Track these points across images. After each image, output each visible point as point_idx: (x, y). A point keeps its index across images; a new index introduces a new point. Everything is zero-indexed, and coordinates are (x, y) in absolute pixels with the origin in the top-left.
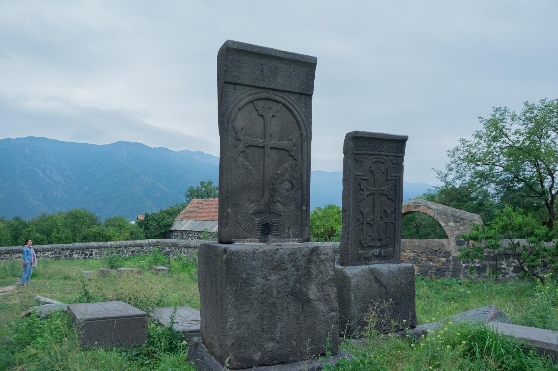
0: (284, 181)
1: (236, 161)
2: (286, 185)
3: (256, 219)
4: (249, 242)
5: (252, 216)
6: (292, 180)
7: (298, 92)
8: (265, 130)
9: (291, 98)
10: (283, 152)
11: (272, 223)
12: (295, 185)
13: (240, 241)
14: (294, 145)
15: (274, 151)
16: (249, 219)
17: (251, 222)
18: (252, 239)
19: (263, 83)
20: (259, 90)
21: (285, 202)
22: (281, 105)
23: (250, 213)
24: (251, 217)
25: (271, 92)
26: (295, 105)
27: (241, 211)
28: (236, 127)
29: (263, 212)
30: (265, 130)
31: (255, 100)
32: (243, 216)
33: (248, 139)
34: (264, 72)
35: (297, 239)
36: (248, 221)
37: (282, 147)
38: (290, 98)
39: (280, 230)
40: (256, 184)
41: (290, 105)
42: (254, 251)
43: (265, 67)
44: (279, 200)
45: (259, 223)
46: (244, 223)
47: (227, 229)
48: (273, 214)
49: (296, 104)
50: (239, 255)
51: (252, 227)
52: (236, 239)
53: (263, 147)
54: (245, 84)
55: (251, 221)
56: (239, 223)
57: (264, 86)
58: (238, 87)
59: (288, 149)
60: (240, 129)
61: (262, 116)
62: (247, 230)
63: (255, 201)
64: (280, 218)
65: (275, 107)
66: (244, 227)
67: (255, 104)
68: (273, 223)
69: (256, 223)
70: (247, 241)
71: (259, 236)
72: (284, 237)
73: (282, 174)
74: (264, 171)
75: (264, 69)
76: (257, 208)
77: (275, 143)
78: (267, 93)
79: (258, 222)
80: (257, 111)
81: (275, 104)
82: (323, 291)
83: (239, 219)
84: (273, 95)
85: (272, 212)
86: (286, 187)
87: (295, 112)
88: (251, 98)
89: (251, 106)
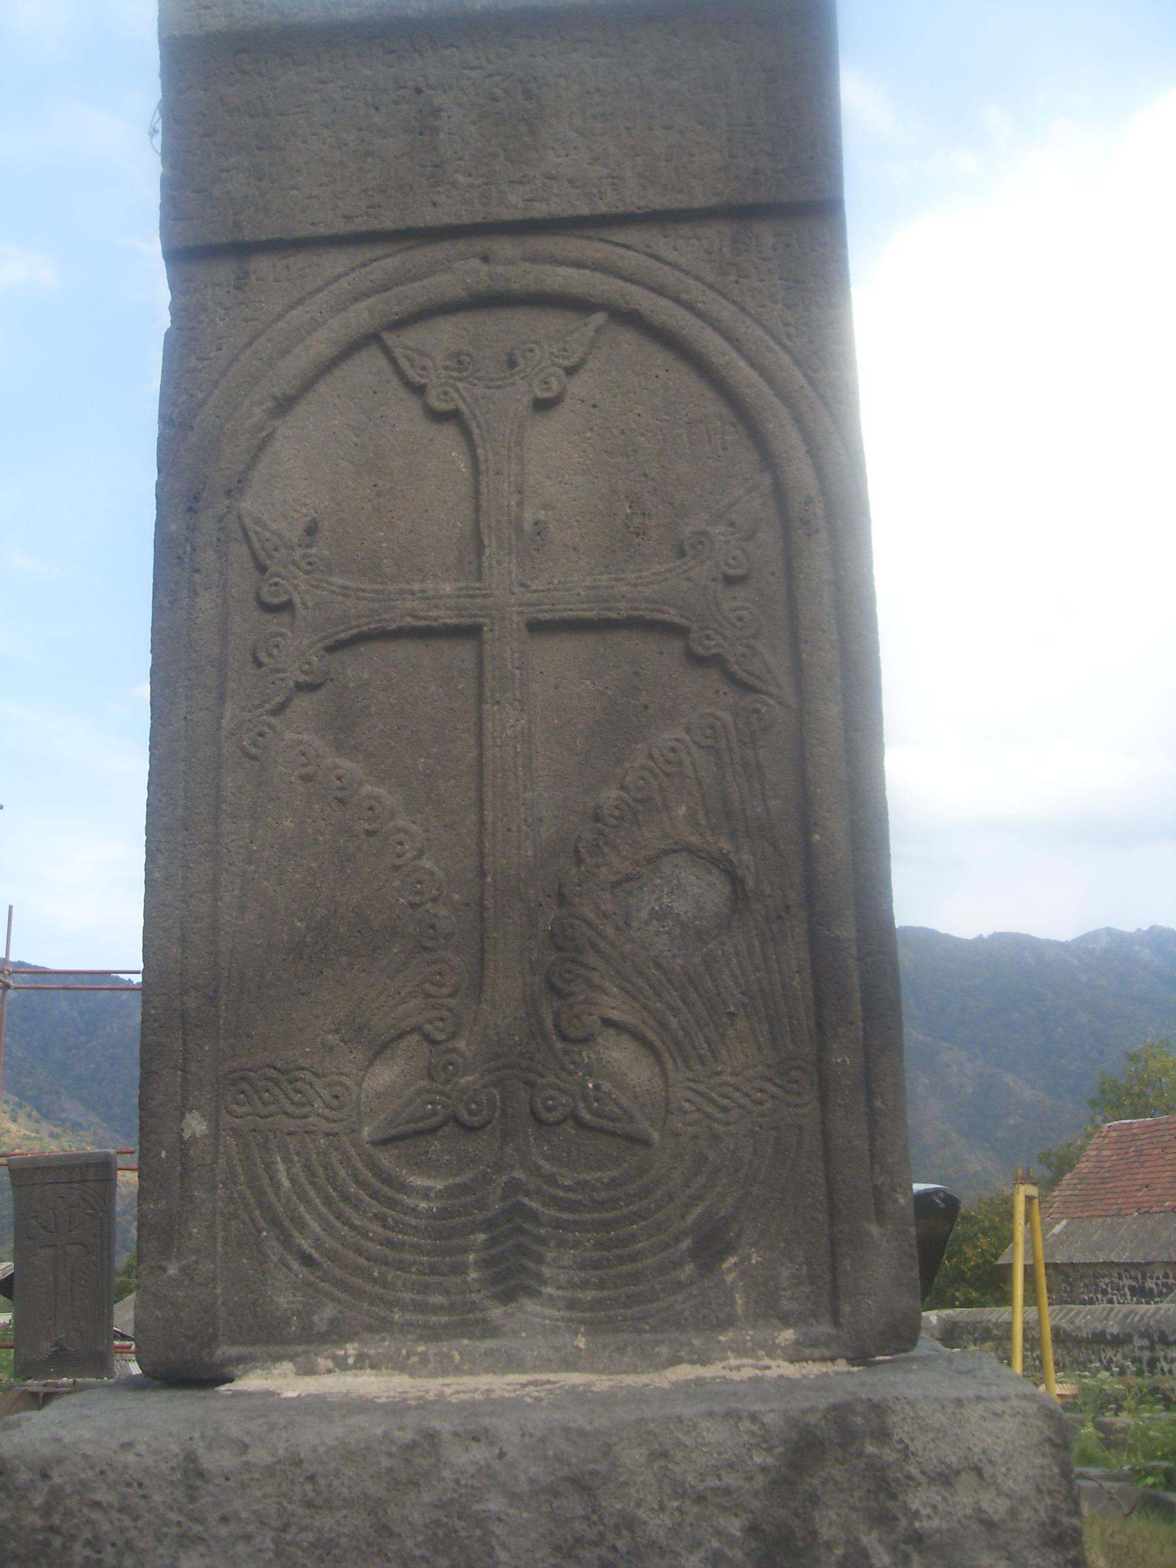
0: (653, 861)
1: (254, 758)
3: (419, 1181)
4: (355, 1367)
5: (385, 1159)
6: (726, 846)
7: (713, 201)
8: (477, 509)
9: (670, 255)
11: (558, 1203)
12: (750, 884)
13: (280, 1358)
14: (730, 581)
15: (568, 647)
16: (362, 1184)
17: (377, 1207)
18: (385, 1345)
19: (442, 199)
20: (420, 256)
21: (664, 1026)
22: (600, 318)
23: (366, 1132)
24: (373, 1166)
25: (504, 247)
27: (292, 1125)
28: (258, 521)
29: (475, 1121)
30: (477, 509)
31: (400, 324)
32: (307, 1167)
33: (345, 592)
34: (436, 130)
35: (787, 1335)
36: (346, 1198)
37: (622, 610)
38: (659, 259)
39: (633, 1258)
40: (413, 905)
41: (665, 303)
42: (191, 1457)
43: (440, 100)
44: (615, 1015)
45: (444, 1214)
46: (321, 1218)
47: (172, 1270)
48: (570, 1128)
49: (711, 286)
50: (56, 1494)
51: (389, 1243)
52: (250, 1349)
53: (470, 632)
54: (305, 231)
55: (375, 1195)
56: (274, 1222)
57: (452, 220)
58: (263, 265)
59: (673, 616)
60: (295, 534)
61: (452, 417)
62: (338, 1273)
63: (415, 1037)
66: (318, 1244)
67: (398, 352)
68: (572, 1206)
69: (414, 1211)
70: (341, 1365)
71: (444, 1319)
74: (480, 804)
75: (436, 112)
76: (419, 1093)
78: (485, 259)
79: (435, 1206)
80: (419, 390)
81: (553, 321)
83: (277, 1186)
84: (526, 266)
85: (551, 1117)
86: (680, 907)
87: (710, 342)
88: (360, 317)
89: (370, 362)
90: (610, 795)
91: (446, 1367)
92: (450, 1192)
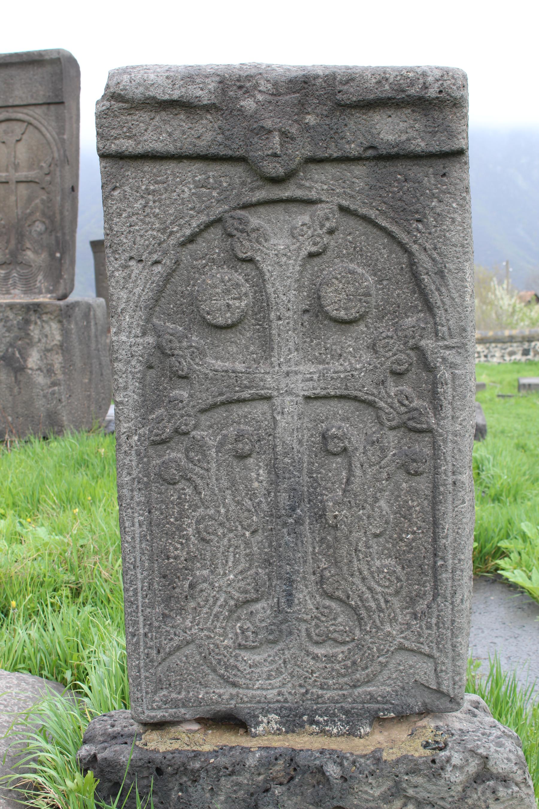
0: (35, 222)
2: (38, 227)
10: (33, 185)
22: (26, 124)
25: (10, 110)
26: (43, 121)
37: (29, 179)
59: (37, 180)
64: (30, 269)
65: (18, 128)
72: (35, 293)
73: (32, 213)
77: (23, 174)
81: (19, 124)
82: (47, 359)
86: (38, 229)
87: (43, 129)
90: (28, 211)
91: (5, 299)
92: (6, 273)
